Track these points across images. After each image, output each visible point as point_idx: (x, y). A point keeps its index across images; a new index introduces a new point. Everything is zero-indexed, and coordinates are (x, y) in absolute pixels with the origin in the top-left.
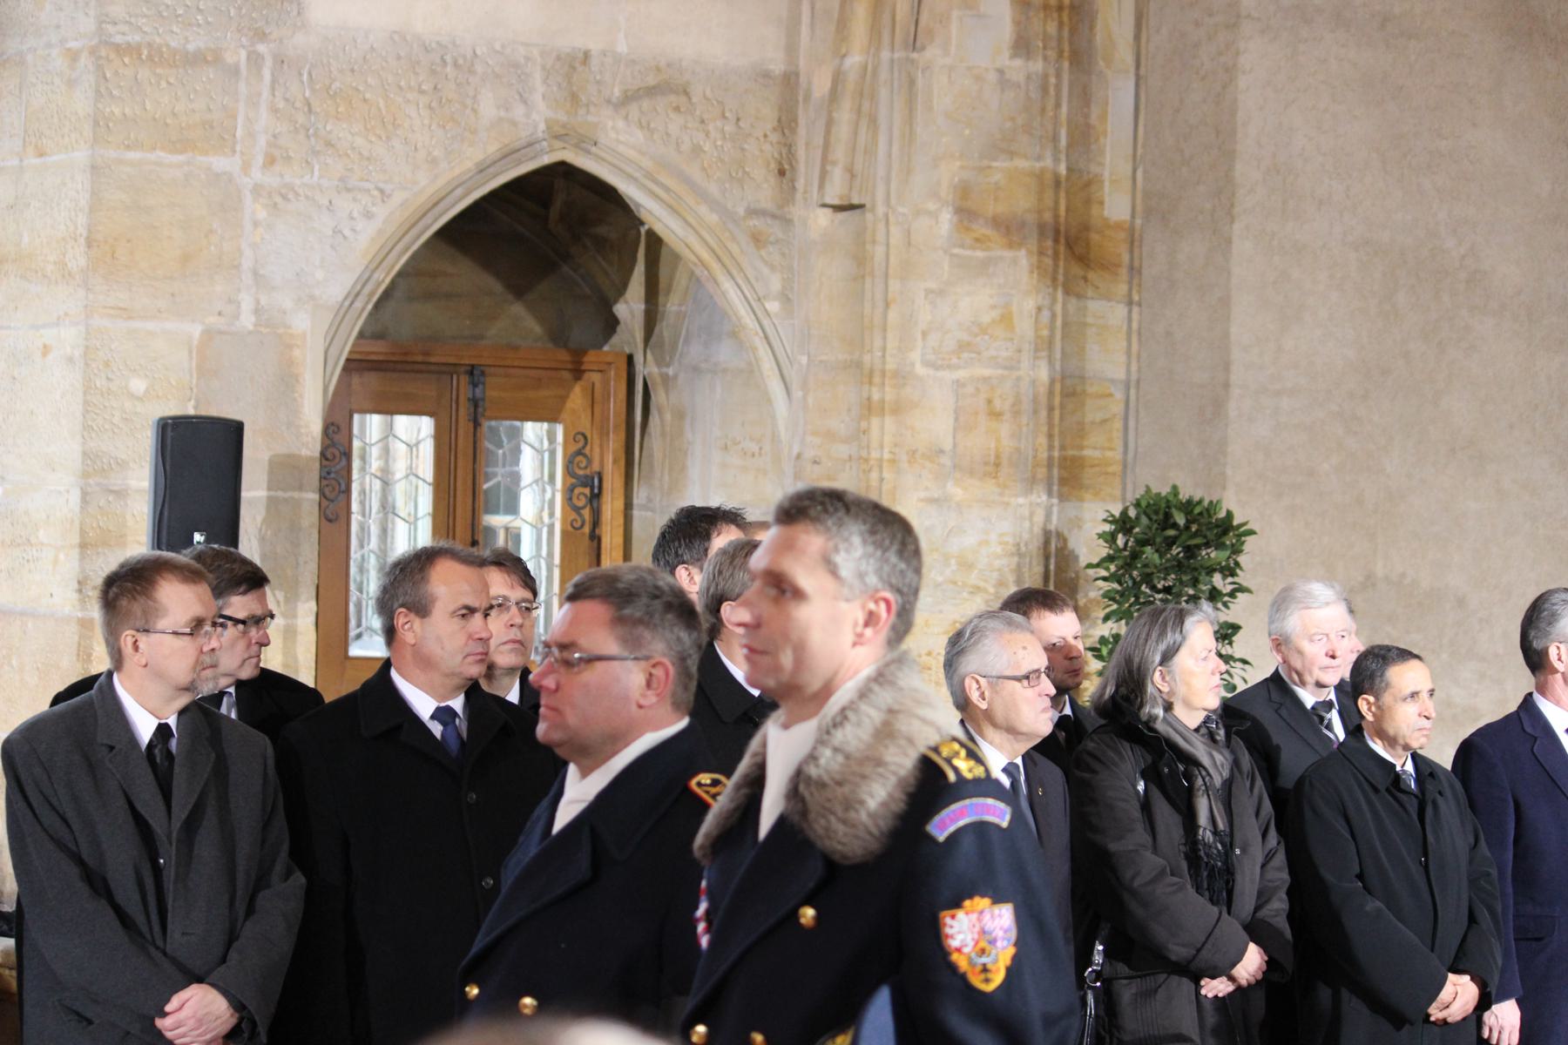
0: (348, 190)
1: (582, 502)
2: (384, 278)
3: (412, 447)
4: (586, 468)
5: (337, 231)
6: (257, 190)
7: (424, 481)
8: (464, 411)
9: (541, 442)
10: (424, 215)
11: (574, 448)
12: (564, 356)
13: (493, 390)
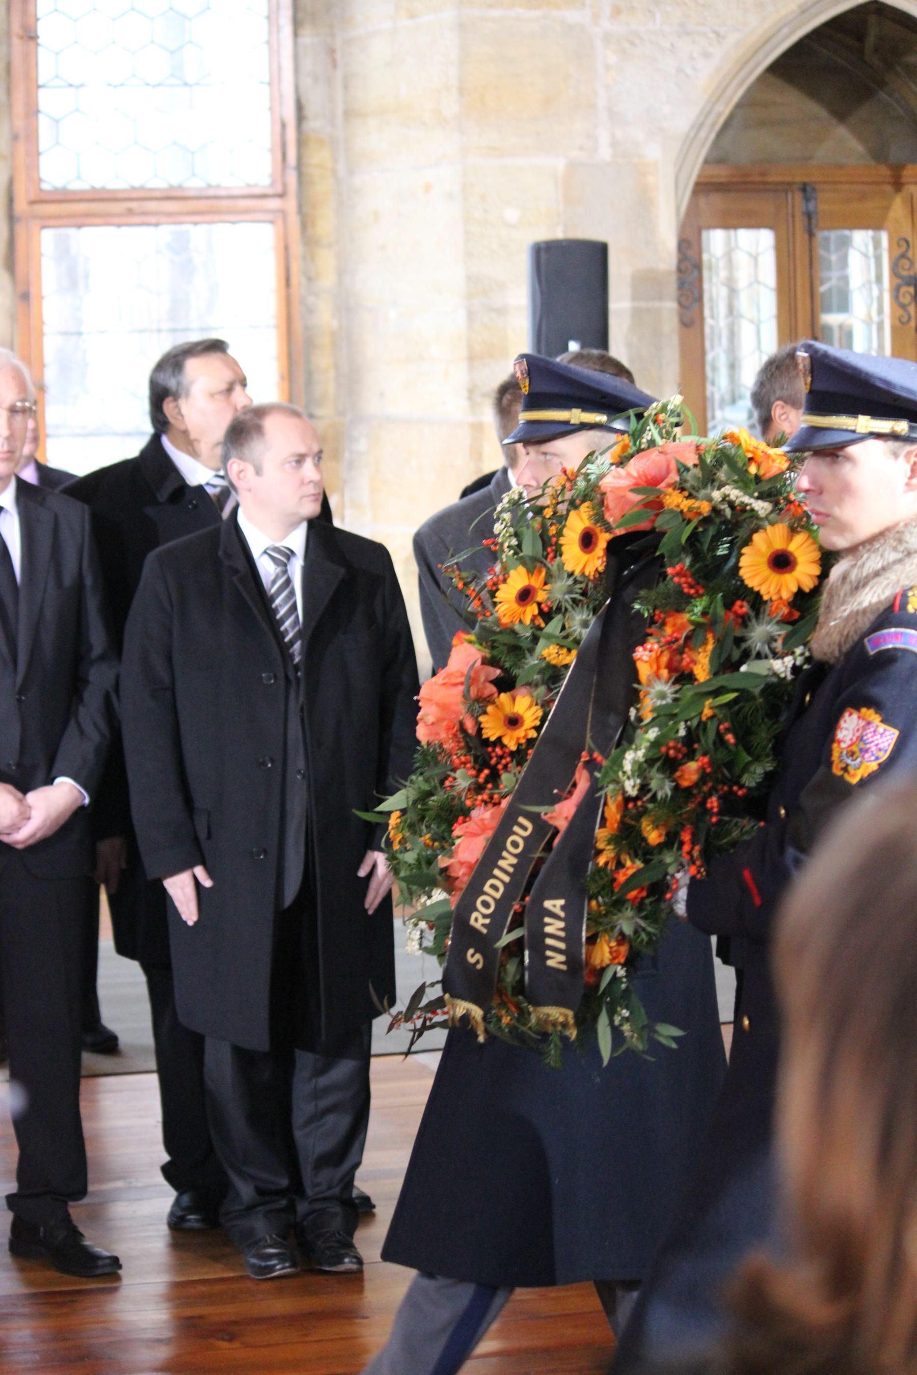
0: (688, 34)
1: (907, 300)
2: (724, 109)
3: (755, 258)
4: (909, 269)
5: (680, 70)
6: (607, 38)
7: (765, 286)
8: (800, 223)
9: (867, 246)
10: (757, 51)
11: (898, 252)
12: (884, 171)
13: (824, 204)
